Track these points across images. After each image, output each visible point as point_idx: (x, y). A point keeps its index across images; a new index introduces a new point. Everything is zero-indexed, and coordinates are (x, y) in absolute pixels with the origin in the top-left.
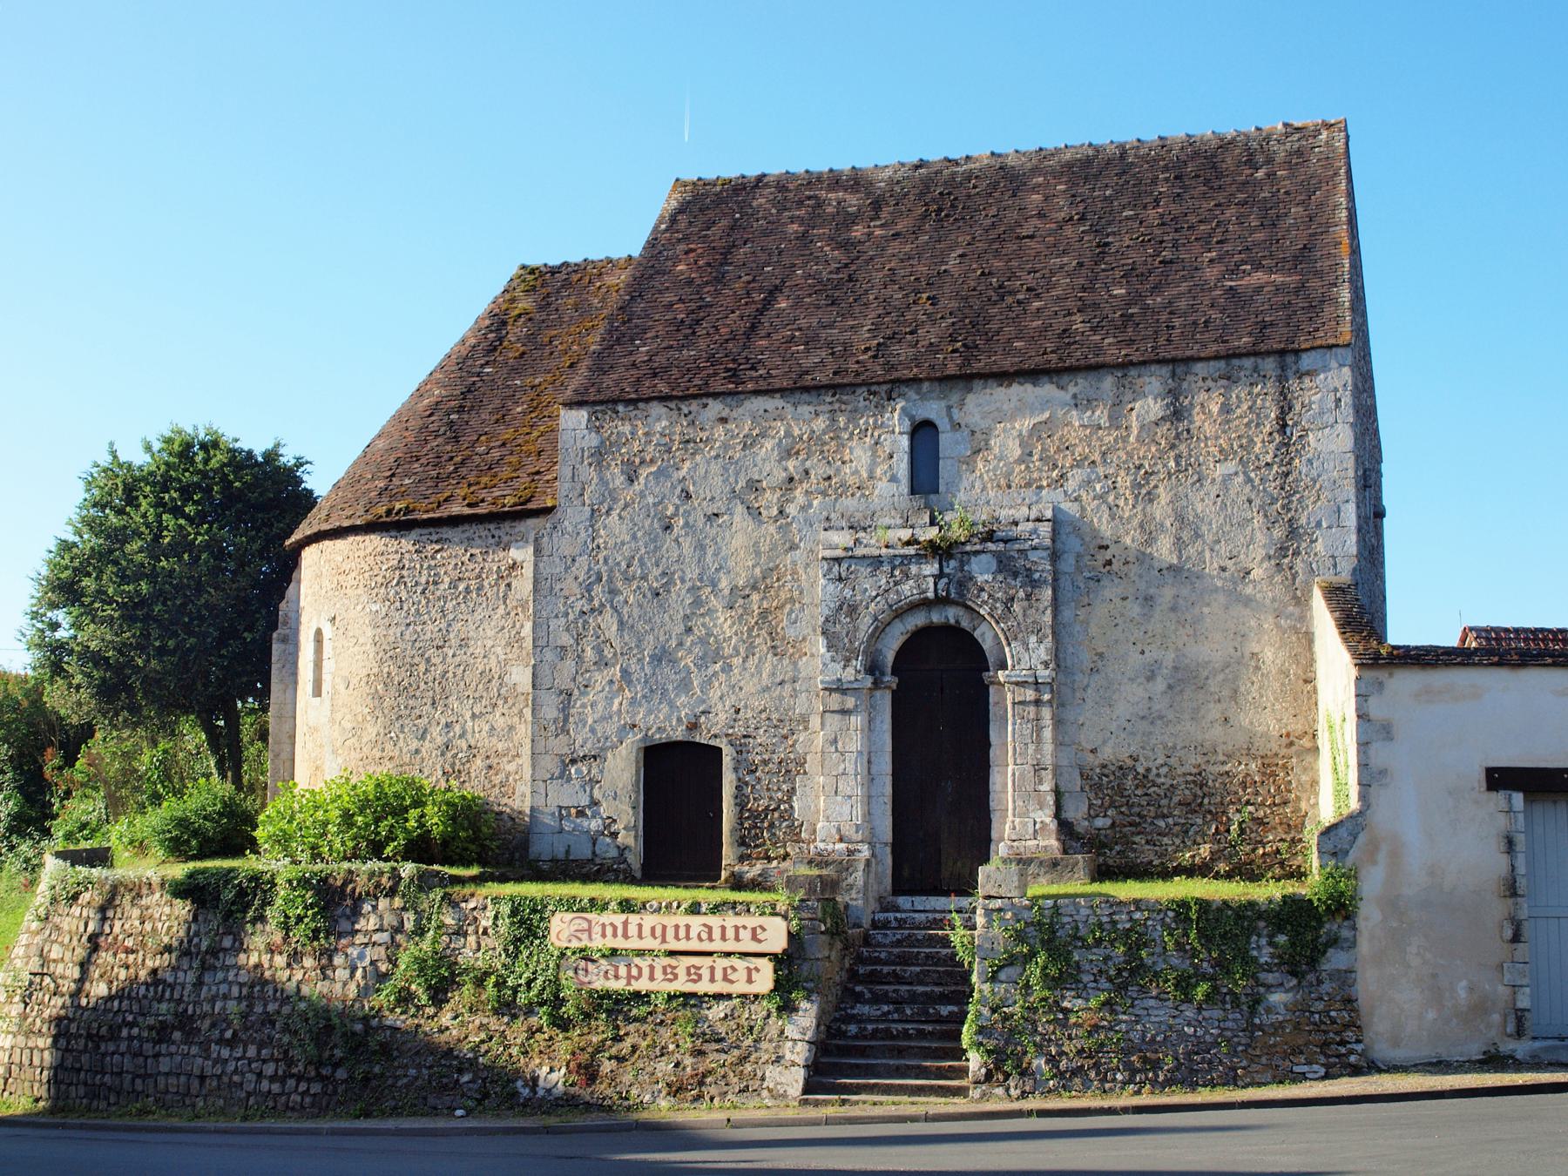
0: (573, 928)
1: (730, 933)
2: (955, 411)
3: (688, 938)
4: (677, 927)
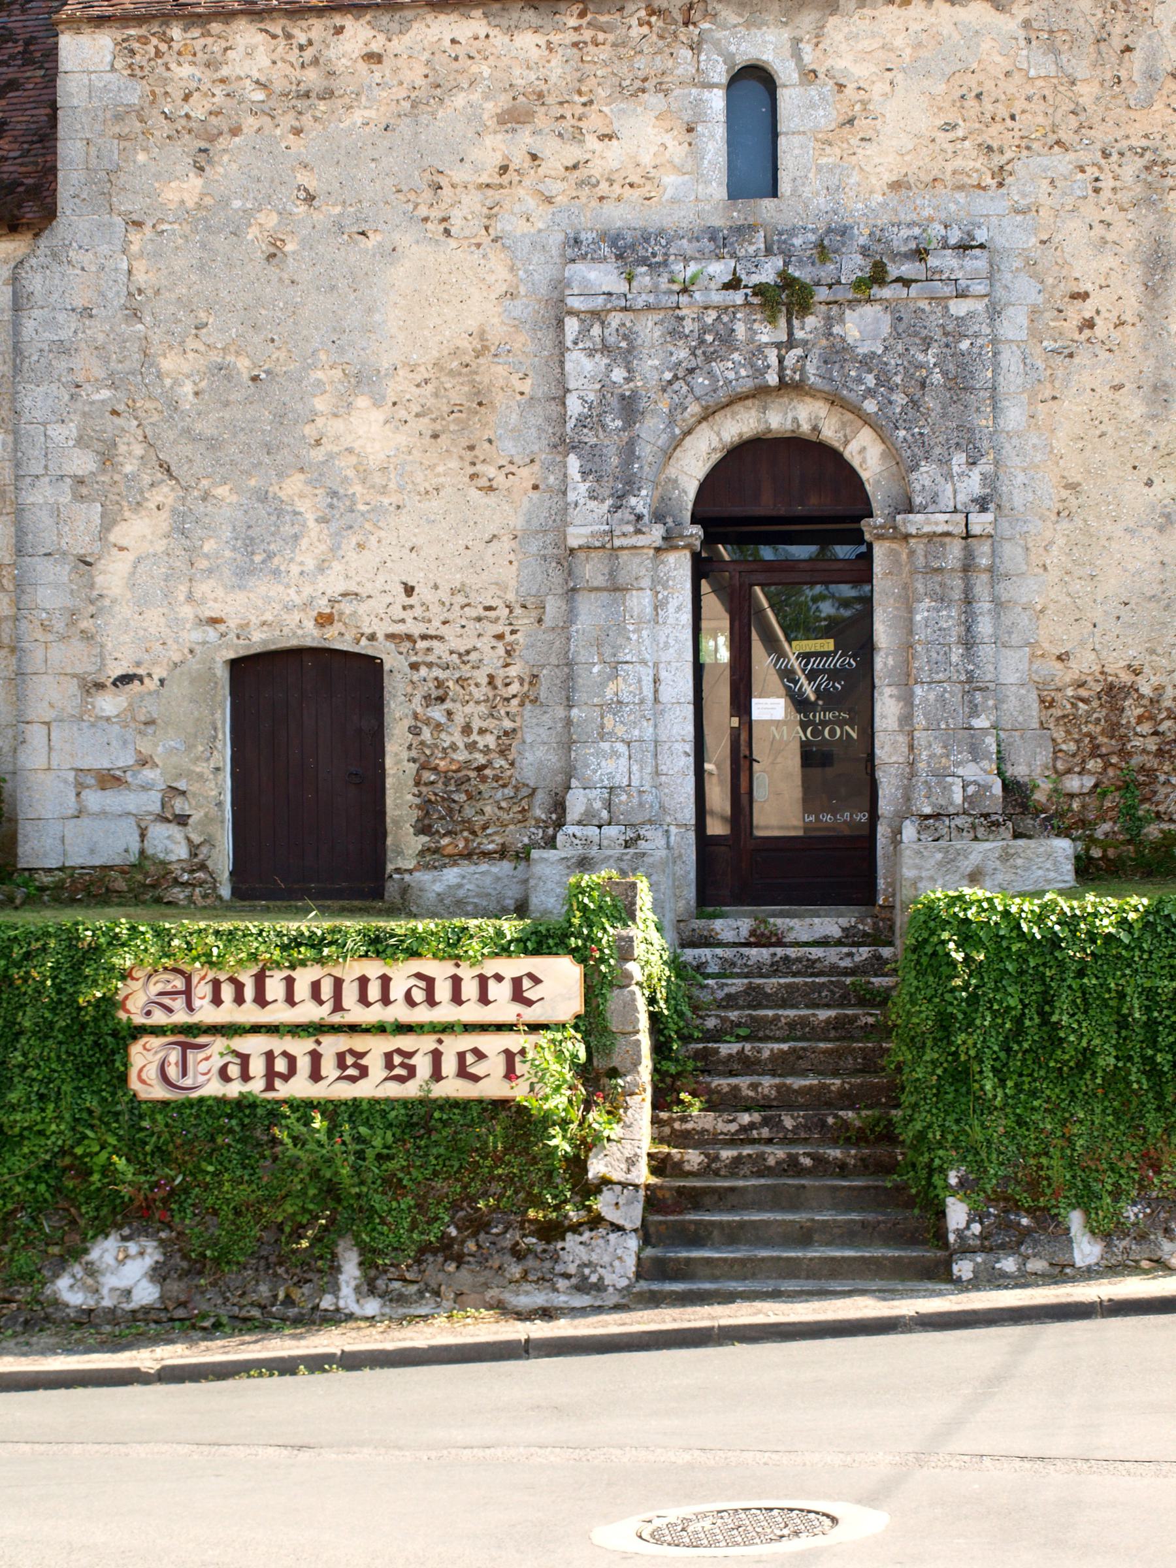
0: (154, 989)
1: (470, 989)
2: (806, 48)
3: (386, 1000)
4: (363, 981)
